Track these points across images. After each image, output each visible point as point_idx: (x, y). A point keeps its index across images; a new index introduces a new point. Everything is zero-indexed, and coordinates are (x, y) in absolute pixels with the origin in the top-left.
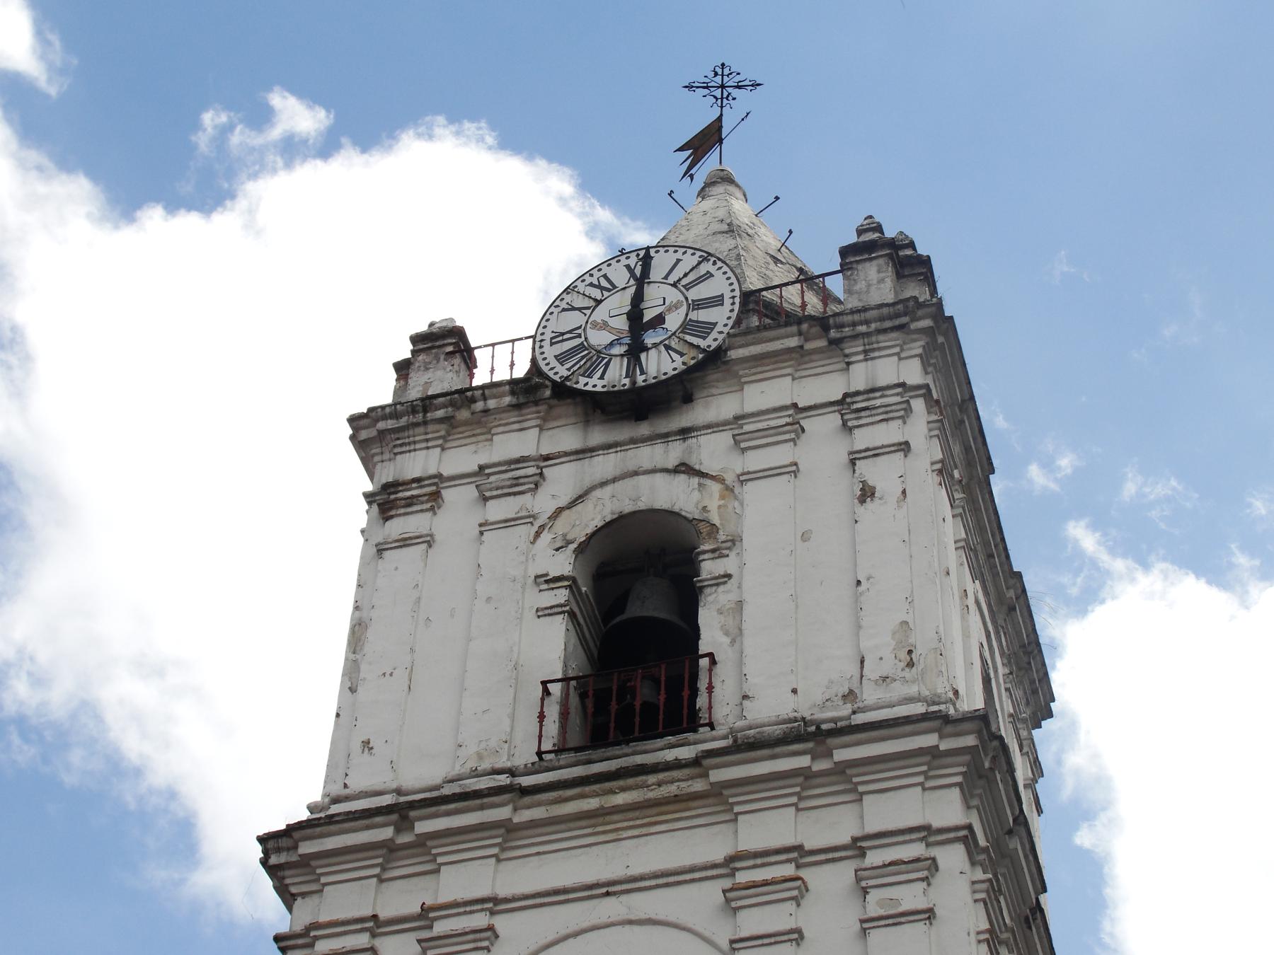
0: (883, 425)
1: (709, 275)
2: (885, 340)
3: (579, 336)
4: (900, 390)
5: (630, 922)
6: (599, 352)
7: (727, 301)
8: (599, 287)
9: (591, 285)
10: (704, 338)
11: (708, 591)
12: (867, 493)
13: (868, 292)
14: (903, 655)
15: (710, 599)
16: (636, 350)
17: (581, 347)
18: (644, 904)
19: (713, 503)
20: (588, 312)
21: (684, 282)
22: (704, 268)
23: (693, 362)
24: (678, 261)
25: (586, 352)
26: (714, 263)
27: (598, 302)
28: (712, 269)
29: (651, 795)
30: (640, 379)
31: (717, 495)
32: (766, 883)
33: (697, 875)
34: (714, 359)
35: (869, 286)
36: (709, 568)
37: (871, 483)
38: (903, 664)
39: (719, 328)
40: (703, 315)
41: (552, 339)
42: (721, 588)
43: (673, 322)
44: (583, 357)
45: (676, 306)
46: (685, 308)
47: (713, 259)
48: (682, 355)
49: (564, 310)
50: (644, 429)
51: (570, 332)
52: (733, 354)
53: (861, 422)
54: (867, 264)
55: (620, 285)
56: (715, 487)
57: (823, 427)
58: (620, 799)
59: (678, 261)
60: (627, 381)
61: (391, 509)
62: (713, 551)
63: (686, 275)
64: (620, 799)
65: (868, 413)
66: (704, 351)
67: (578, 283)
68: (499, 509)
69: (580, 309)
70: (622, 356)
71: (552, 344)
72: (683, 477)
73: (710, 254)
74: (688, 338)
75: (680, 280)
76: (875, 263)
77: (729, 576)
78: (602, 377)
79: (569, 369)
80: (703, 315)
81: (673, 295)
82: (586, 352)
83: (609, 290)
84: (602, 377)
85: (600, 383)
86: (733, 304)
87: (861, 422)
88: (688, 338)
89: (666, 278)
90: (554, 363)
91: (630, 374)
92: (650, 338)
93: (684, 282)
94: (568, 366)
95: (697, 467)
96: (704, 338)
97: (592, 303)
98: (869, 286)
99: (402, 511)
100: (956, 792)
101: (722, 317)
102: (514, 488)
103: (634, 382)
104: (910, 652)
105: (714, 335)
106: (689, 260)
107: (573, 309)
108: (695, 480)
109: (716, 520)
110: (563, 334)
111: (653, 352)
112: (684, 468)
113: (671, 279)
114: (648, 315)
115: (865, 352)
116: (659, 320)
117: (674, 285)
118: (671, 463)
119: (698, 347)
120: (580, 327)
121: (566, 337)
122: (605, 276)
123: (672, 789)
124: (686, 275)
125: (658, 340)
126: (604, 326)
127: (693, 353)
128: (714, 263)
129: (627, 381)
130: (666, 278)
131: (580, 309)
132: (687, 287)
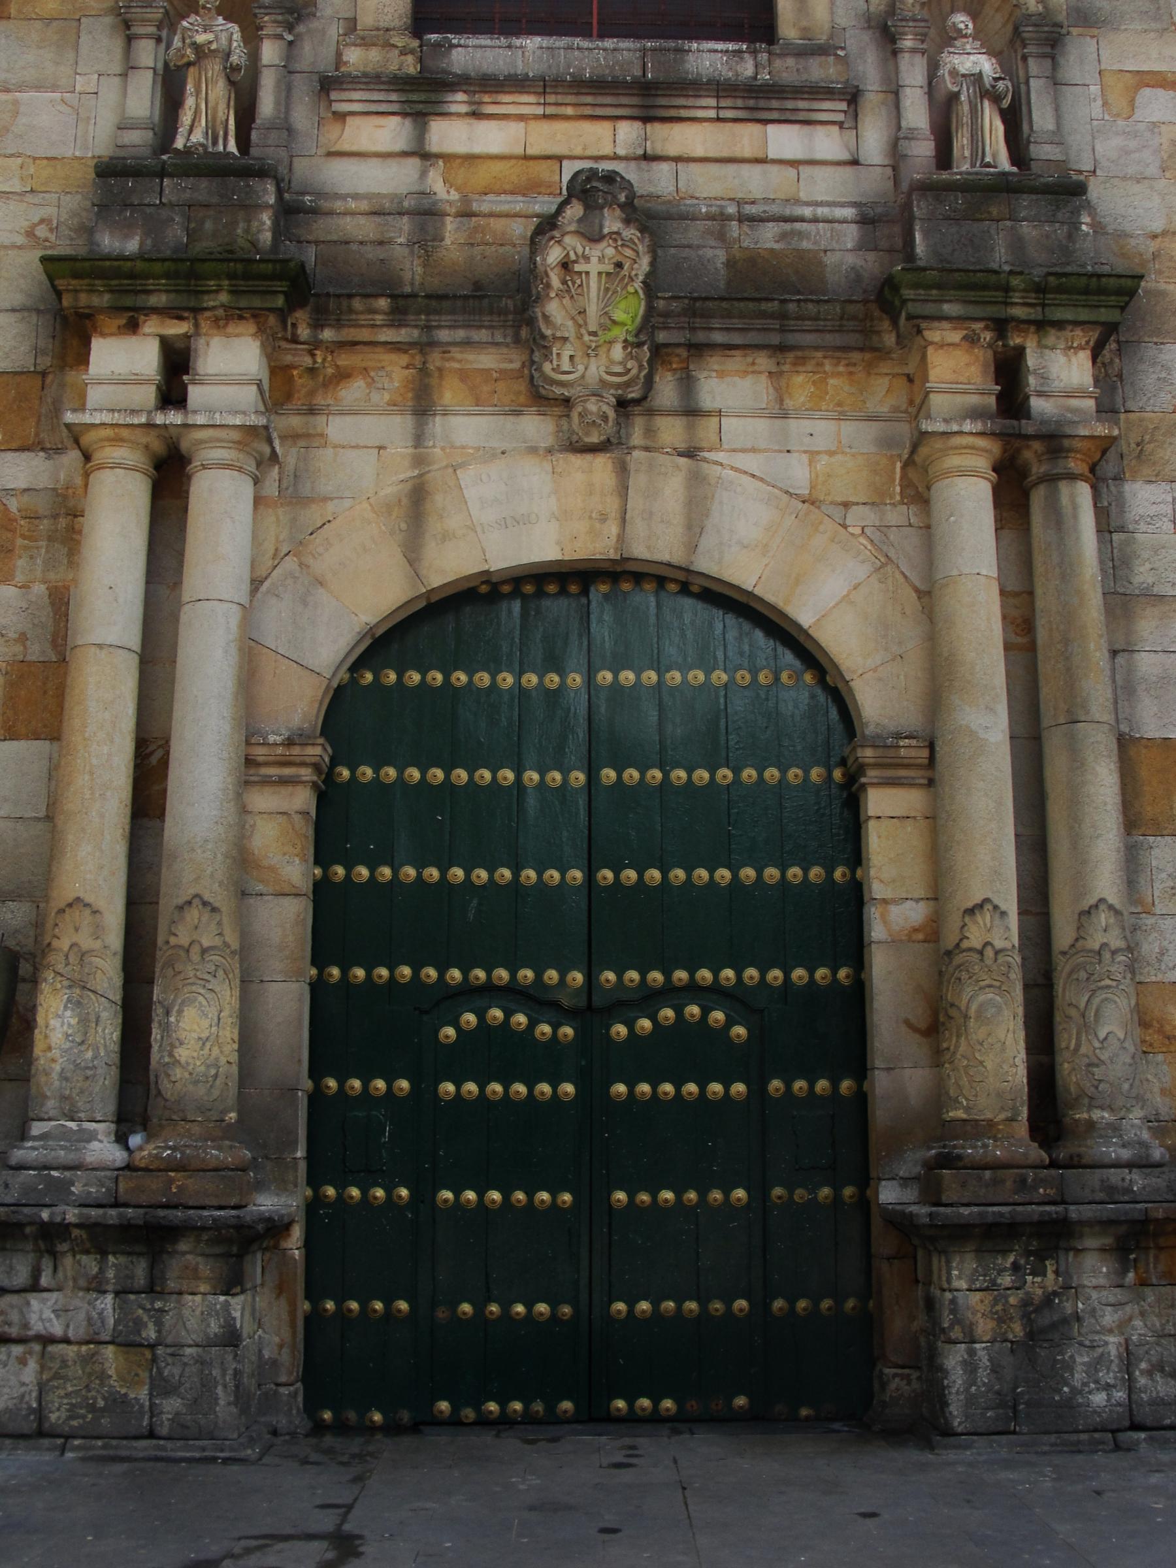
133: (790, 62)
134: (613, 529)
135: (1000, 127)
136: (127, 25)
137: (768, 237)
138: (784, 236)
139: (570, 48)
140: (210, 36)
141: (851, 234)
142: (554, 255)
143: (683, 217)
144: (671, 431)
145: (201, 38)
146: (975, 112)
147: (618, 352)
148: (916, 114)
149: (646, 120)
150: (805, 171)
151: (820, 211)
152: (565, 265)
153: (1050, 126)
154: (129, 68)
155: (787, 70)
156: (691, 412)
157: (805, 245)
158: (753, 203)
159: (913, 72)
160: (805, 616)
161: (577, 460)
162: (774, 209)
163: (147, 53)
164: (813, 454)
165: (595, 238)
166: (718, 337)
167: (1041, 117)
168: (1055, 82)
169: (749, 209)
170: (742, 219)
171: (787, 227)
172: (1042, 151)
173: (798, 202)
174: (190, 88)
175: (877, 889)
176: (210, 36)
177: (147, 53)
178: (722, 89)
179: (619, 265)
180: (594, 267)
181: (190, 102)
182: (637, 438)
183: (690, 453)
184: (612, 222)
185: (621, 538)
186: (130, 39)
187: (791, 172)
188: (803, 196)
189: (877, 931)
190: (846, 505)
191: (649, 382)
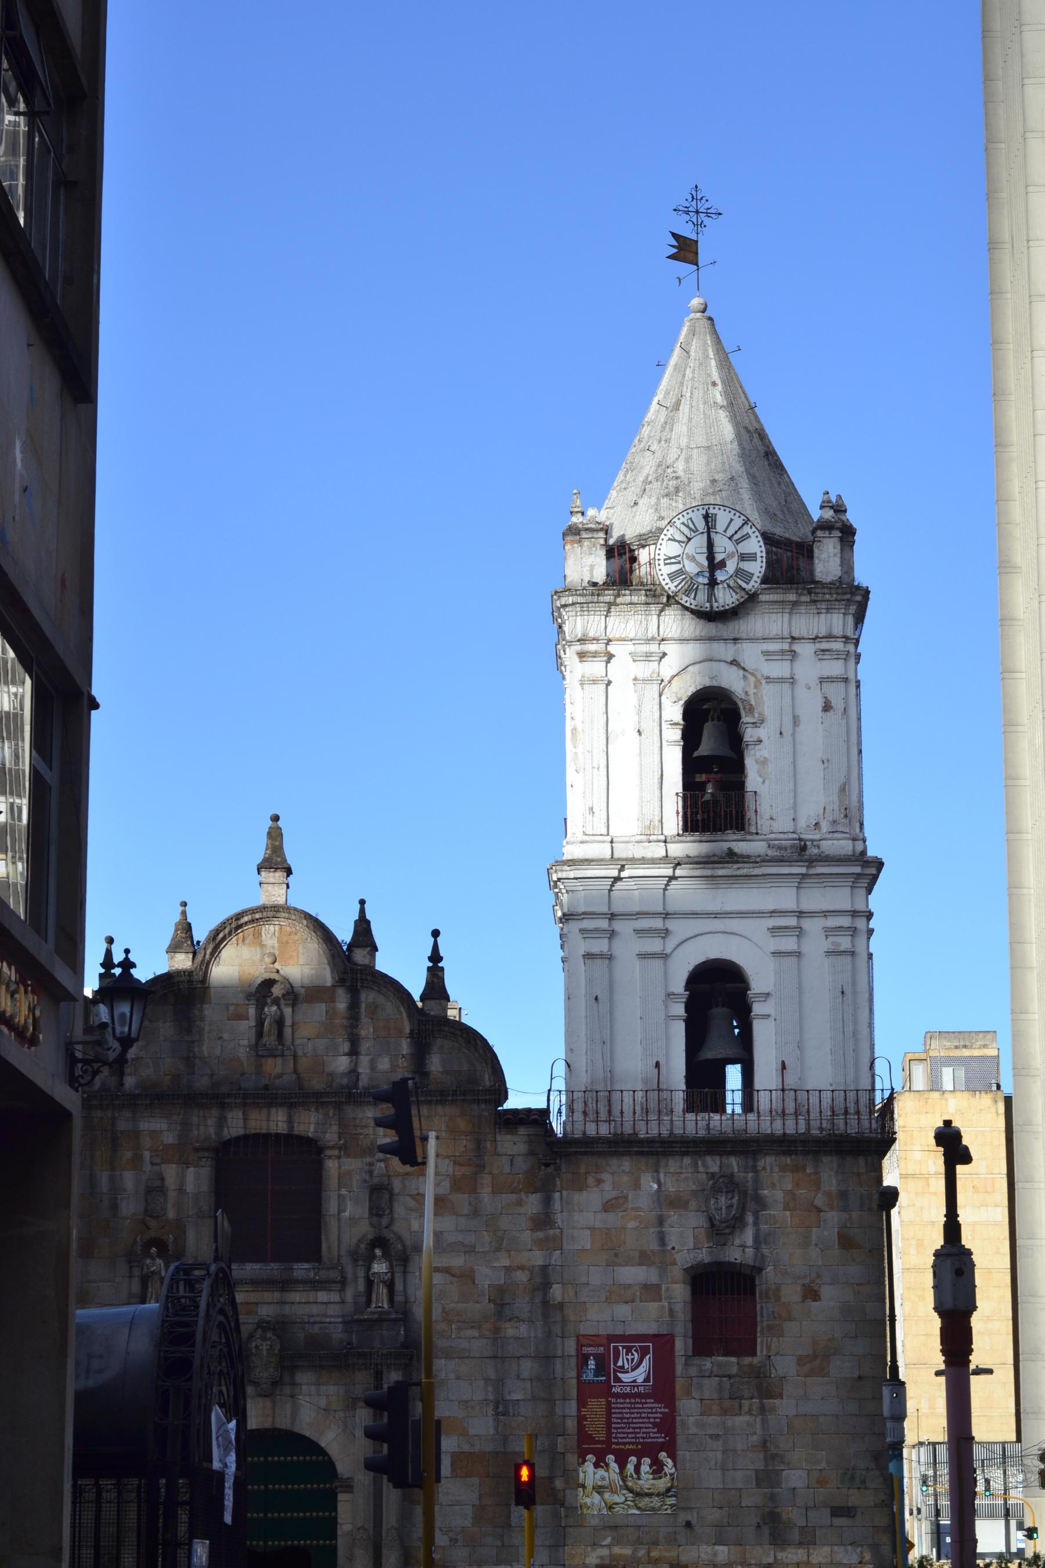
0: (835, 661)
1: (747, 537)
2: (837, 605)
3: (679, 563)
4: (844, 640)
5: (726, 933)
6: (691, 578)
7: (759, 559)
8: (688, 526)
9: (683, 523)
10: (748, 584)
11: (750, 747)
12: (827, 707)
13: (828, 561)
14: (843, 811)
15: (752, 752)
16: (713, 583)
17: (681, 572)
18: (733, 924)
19: (752, 691)
20: (683, 545)
21: (736, 537)
22: (747, 529)
23: (743, 600)
24: (732, 520)
25: (684, 576)
26: (751, 528)
27: (689, 539)
28: (750, 532)
29: (735, 873)
30: (715, 605)
31: (752, 685)
32: (786, 927)
33: (754, 915)
34: (752, 598)
35: (829, 557)
36: (749, 734)
37: (829, 698)
38: (842, 815)
39: (755, 578)
40: (747, 566)
41: (665, 560)
42: (757, 747)
43: (731, 566)
44: (683, 579)
45: (731, 556)
46: (736, 557)
47: (750, 524)
48: (737, 593)
49: (669, 539)
50: (711, 628)
51: (674, 557)
52: (762, 598)
53: (825, 657)
54: (828, 540)
55: (701, 530)
56: (752, 679)
57: (806, 650)
58: (720, 872)
59: (732, 520)
60: (708, 605)
61: (584, 657)
62: (753, 723)
63: (736, 532)
64: (720, 872)
65: (828, 653)
66: (747, 593)
67: (676, 520)
68: (644, 670)
69: (679, 542)
70: (705, 584)
71: (665, 564)
72: (734, 668)
73: (748, 520)
74: (739, 581)
75: (733, 535)
76: (832, 539)
77: (761, 741)
78: (694, 599)
79: (676, 587)
80: (747, 566)
81: (730, 547)
82: (684, 576)
83: (694, 532)
84: (694, 599)
85: (694, 603)
86: (762, 562)
87: (825, 657)
88: (739, 581)
89: (725, 531)
90: (668, 580)
91: (709, 600)
92: (720, 576)
93: (736, 537)
94: (676, 584)
95: (742, 664)
96: (748, 584)
97: (685, 540)
98: (829, 557)
99: (590, 659)
100: (864, 889)
101: (757, 568)
102: (648, 656)
103: (712, 607)
104: (846, 809)
105: (752, 583)
106: (738, 522)
107: (674, 540)
108: (741, 672)
109: (753, 703)
110: (670, 558)
111: (720, 586)
112: (734, 663)
113: (729, 533)
114: (719, 558)
115: (828, 609)
116: (722, 564)
117: (730, 538)
118: (729, 659)
119: (744, 589)
120: (679, 556)
121: (673, 560)
122: (691, 519)
123: (744, 872)
124: (736, 532)
125: (723, 579)
126: (693, 559)
127: (743, 594)
128: (751, 528)
129: (708, 605)
130: (725, 531)
131: (679, 542)
132: (738, 542)
133: (324, 1272)
134: (270, 1420)
135: (385, 1291)
136: (130, 1262)
137: (316, 1329)
138: (320, 1328)
139: (260, 1269)
140: (155, 1268)
141: (340, 1327)
142: (254, 1344)
143: (293, 1323)
144: (287, 1390)
145: (153, 1269)
146: (378, 1288)
147: (271, 1370)
148: (361, 1286)
149: (283, 1291)
150: (329, 1305)
151: (332, 1320)
152: (257, 1347)
153: (401, 1289)
154: (131, 1277)
155: (323, 1274)
156: (293, 1384)
157: (327, 1331)
158: (313, 1316)
159: (361, 1273)
160: (323, 1444)
161: (260, 1400)
162: (318, 1319)
163: (136, 1272)
164: (328, 1396)
165: (265, 1339)
166: (300, 1363)
167: (399, 1286)
168: (405, 1273)
169: (312, 1320)
170: (309, 1323)
171: (322, 1325)
172: (399, 1298)
173: (326, 1316)
174: (150, 1285)
175: (339, 1521)
176: (155, 1268)
177: (136, 1272)
178: (304, 1282)
179: (271, 1346)
180: (264, 1348)
181: (150, 1289)
182: (277, 1392)
183: (292, 1396)
184: (269, 1335)
185: (273, 1422)
186: (131, 1267)
187: (324, 1306)
188: (328, 1314)
189: (339, 1532)
190: (336, 1411)
191: (281, 1376)
